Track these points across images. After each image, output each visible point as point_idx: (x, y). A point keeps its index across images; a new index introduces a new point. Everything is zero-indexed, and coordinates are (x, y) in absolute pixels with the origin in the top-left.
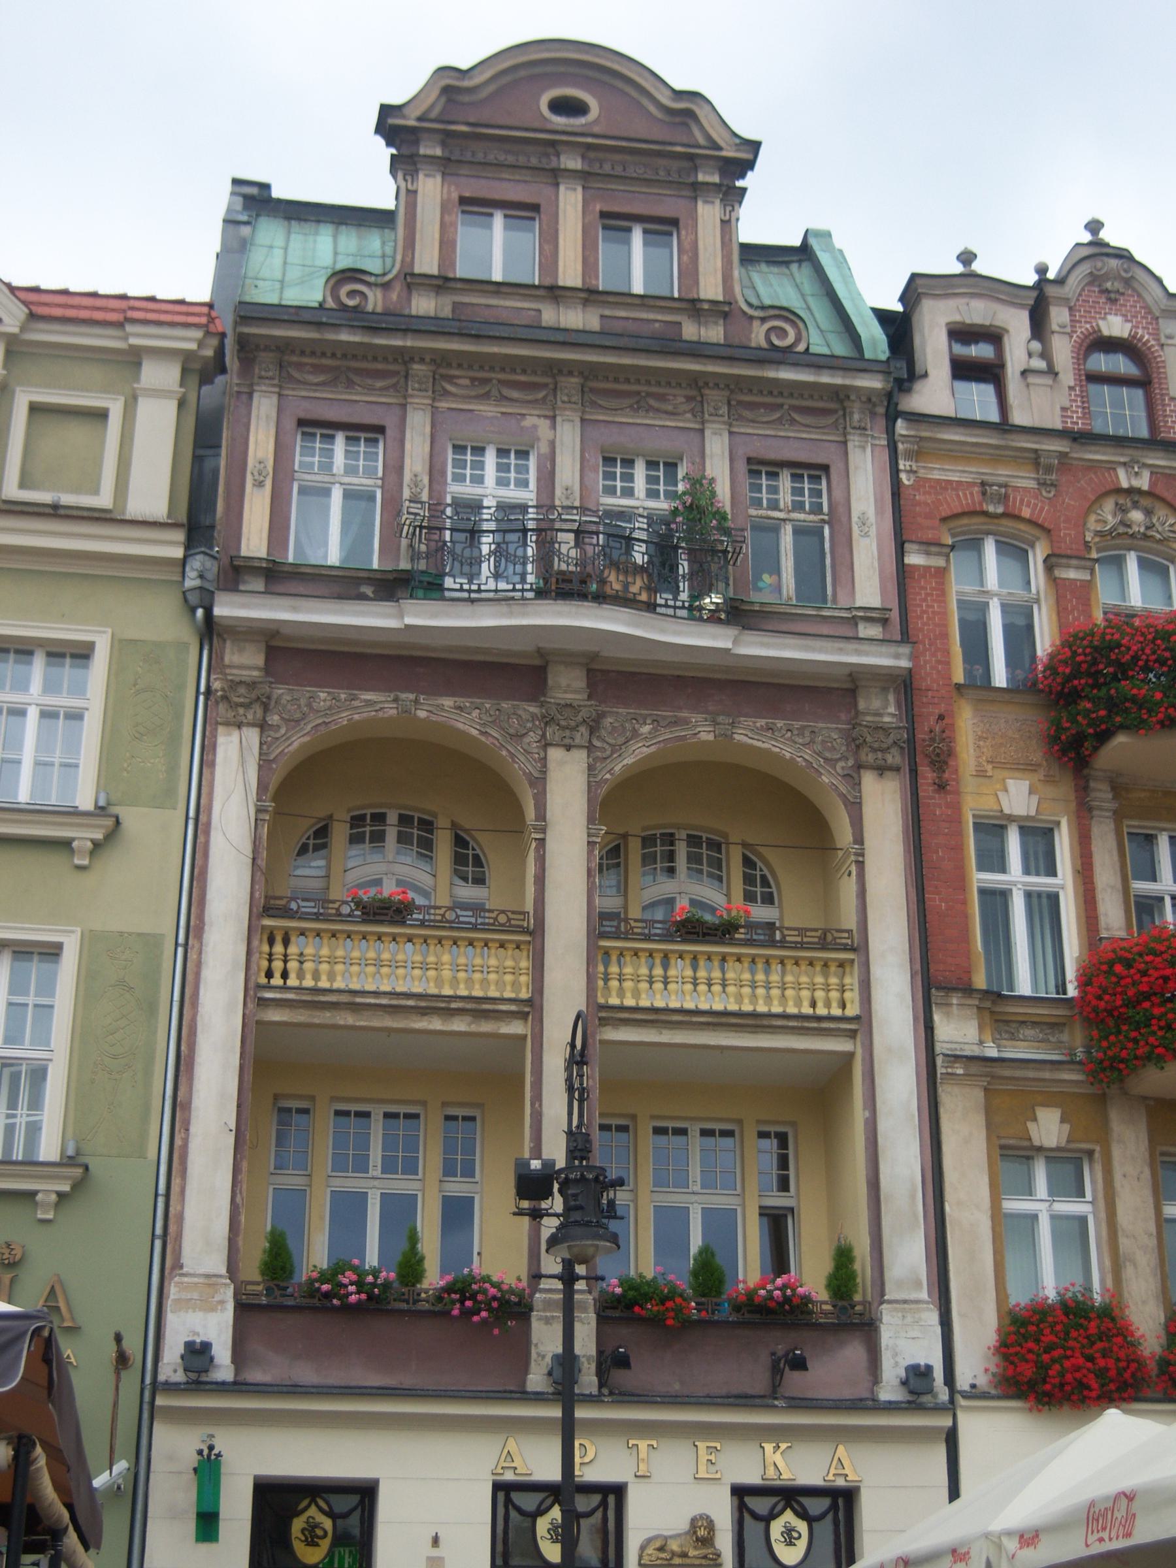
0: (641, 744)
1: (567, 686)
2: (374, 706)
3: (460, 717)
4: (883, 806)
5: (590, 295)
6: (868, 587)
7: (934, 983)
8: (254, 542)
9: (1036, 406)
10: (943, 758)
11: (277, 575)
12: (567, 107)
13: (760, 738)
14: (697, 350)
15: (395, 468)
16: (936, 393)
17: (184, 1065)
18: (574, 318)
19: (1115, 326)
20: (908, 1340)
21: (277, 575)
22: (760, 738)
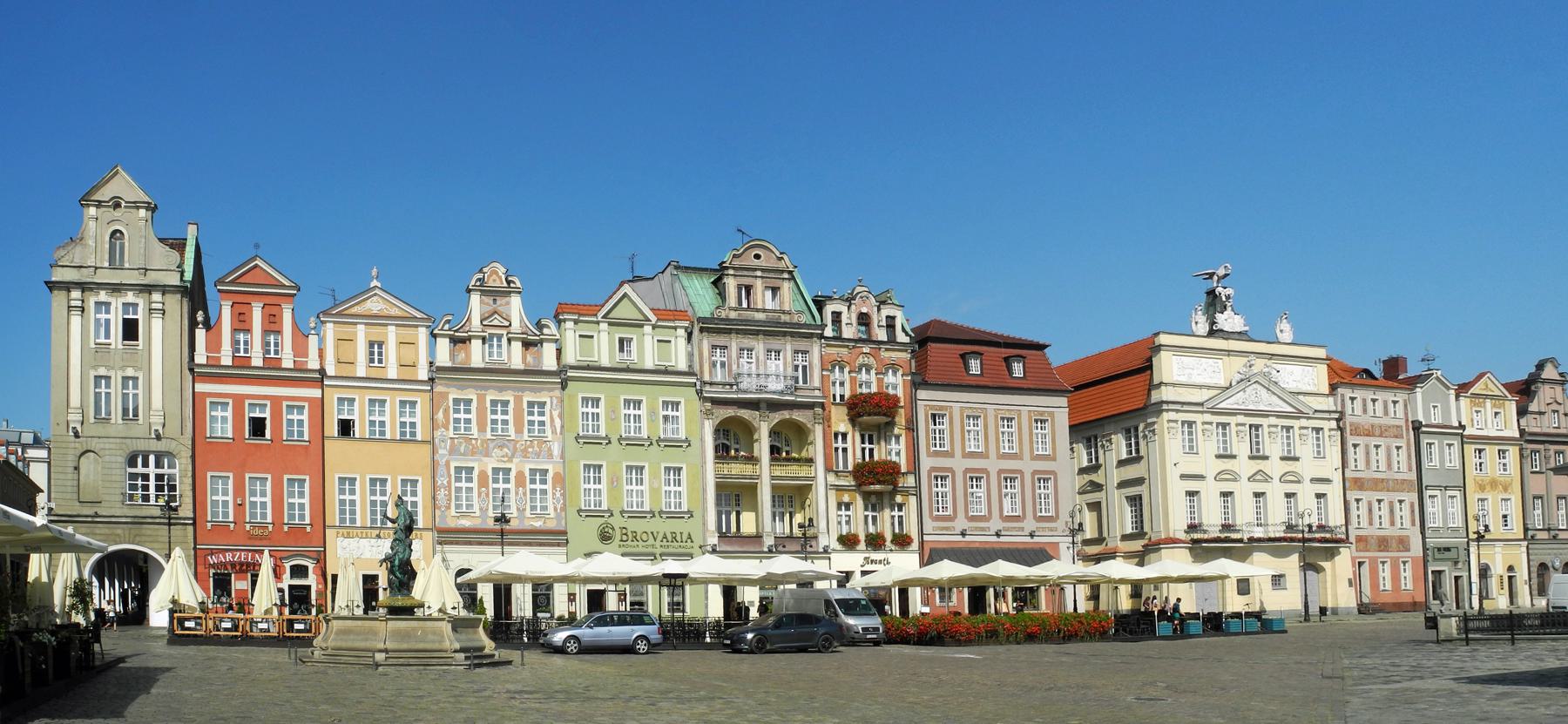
0: (777, 417)
1: (763, 405)
2: (730, 412)
3: (745, 414)
4: (819, 430)
5: (764, 311)
6: (817, 383)
7: (828, 469)
8: (707, 378)
9: (848, 332)
10: (829, 420)
11: (711, 384)
12: (757, 257)
13: (797, 416)
14: (785, 324)
15: (730, 357)
16: (829, 332)
17: (704, 490)
18: (761, 316)
19: (864, 310)
20: (823, 541)
21: (711, 384)
22: (797, 416)
